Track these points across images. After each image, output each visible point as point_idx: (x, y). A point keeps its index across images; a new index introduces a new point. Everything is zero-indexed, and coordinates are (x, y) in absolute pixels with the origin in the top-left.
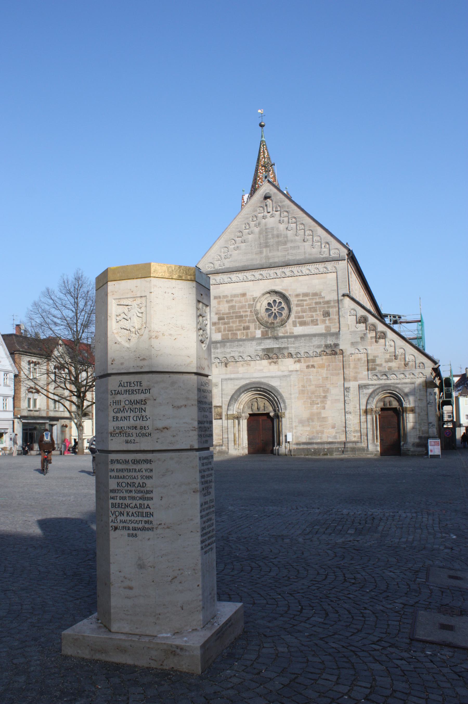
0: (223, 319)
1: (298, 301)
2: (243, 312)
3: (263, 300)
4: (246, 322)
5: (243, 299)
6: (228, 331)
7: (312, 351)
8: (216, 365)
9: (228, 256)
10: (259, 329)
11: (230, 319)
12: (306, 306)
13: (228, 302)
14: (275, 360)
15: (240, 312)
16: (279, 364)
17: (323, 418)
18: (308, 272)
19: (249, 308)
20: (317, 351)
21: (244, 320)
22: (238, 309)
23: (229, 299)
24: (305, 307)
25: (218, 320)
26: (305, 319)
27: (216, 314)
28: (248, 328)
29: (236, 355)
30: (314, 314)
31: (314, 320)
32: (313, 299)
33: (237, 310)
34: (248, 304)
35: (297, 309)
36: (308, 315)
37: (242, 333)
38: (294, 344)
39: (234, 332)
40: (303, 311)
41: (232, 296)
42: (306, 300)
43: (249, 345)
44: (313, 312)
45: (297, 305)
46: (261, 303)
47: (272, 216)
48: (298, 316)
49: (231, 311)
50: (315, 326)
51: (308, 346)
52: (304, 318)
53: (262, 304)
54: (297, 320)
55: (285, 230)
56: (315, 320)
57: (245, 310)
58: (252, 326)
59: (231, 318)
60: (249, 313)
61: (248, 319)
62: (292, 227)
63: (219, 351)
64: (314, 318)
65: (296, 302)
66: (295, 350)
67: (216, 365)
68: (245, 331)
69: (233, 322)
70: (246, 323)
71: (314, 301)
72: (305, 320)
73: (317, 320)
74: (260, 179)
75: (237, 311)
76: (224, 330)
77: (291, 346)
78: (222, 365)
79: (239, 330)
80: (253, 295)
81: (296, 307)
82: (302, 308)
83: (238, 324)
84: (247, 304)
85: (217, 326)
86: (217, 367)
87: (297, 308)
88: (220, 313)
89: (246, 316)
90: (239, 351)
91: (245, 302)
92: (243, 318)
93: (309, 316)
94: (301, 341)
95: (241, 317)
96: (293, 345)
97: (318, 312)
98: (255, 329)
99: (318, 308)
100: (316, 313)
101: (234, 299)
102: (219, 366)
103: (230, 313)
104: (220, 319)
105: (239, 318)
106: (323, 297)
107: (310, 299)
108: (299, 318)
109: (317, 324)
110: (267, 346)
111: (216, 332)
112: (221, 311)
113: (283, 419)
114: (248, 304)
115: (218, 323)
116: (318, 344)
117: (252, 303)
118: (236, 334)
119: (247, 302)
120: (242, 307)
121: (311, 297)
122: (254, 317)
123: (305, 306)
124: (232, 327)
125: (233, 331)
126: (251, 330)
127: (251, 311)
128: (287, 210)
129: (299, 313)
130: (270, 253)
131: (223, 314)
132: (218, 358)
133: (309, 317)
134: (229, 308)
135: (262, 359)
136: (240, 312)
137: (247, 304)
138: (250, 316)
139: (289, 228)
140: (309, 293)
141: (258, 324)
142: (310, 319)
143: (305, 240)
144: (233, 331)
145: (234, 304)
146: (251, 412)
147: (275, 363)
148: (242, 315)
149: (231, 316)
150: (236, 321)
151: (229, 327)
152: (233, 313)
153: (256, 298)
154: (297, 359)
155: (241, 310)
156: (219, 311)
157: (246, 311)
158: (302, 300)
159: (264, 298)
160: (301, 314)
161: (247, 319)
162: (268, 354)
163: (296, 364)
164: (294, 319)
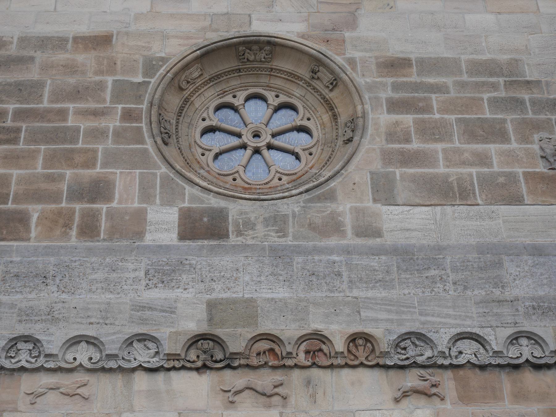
1: (396, 87)
3: (199, 82)
4: (95, 159)
7: (510, 331)
10: (168, 202)
12: (444, 110)
15: (62, 114)
16: (292, 400)
19: (117, 97)
21: (80, 151)
22: (51, 101)
24: (437, 116)
26: (441, 170)
30: (493, 148)
32: (478, 86)
33: (45, 104)
34: (115, 81)
35: (397, 123)
36: (457, 151)
37: (59, 213)
38: (386, 284)
39: (10, 206)
41: (24, 41)
43: (99, 275)
44: (486, 141)
46: (186, 93)
48: (402, 153)
50: (504, 209)
52: (433, 163)
53: (186, 100)
56: (501, 180)
57: (92, 105)
61: (106, 151)
64: (496, 169)
66: (400, 323)
68: (78, 207)
70: (90, 163)
71: (486, 96)
72: (447, 176)
73: (511, 178)
75: (49, 111)
77: (370, 294)
80: (149, 49)
81: (389, 111)
82: (423, 121)
83: (40, 170)
84: (110, 80)
87: (395, 117)
91: (100, 72)
92: (74, 140)
93: (466, 155)
94: (433, 272)
96: (380, 293)
97: (514, 145)
99: (510, 127)
100: (505, 147)
101: (39, 56)
105: (47, 143)
106: (528, 82)
107: (462, 85)
109: (517, 200)
110: (218, 286)
114: (115, 81)
116: (541, 293)
117: (139, 79)
121: (465, 78)
122: (142, 142)
126: (114, 204)
127: (128, 115)
129: (408, 140)
133: (464, 163)
136: (62, 114)
137: (110, 80)
138: (118, 135)
140: (456, 62)
141: (165, 180)
142: (474, 171)
148: (78, 130)
149: (8, 130)
150: (32, 155)
152: (19, 115)
153: (164, 60)
155: (71, 106)
157: (96, 114)
158: (416, 87)
159: (207, 76)
160: (415, 145)
161: (100, 147)
162: (219, 332)
163: (405, 403)
164: (377, 166)
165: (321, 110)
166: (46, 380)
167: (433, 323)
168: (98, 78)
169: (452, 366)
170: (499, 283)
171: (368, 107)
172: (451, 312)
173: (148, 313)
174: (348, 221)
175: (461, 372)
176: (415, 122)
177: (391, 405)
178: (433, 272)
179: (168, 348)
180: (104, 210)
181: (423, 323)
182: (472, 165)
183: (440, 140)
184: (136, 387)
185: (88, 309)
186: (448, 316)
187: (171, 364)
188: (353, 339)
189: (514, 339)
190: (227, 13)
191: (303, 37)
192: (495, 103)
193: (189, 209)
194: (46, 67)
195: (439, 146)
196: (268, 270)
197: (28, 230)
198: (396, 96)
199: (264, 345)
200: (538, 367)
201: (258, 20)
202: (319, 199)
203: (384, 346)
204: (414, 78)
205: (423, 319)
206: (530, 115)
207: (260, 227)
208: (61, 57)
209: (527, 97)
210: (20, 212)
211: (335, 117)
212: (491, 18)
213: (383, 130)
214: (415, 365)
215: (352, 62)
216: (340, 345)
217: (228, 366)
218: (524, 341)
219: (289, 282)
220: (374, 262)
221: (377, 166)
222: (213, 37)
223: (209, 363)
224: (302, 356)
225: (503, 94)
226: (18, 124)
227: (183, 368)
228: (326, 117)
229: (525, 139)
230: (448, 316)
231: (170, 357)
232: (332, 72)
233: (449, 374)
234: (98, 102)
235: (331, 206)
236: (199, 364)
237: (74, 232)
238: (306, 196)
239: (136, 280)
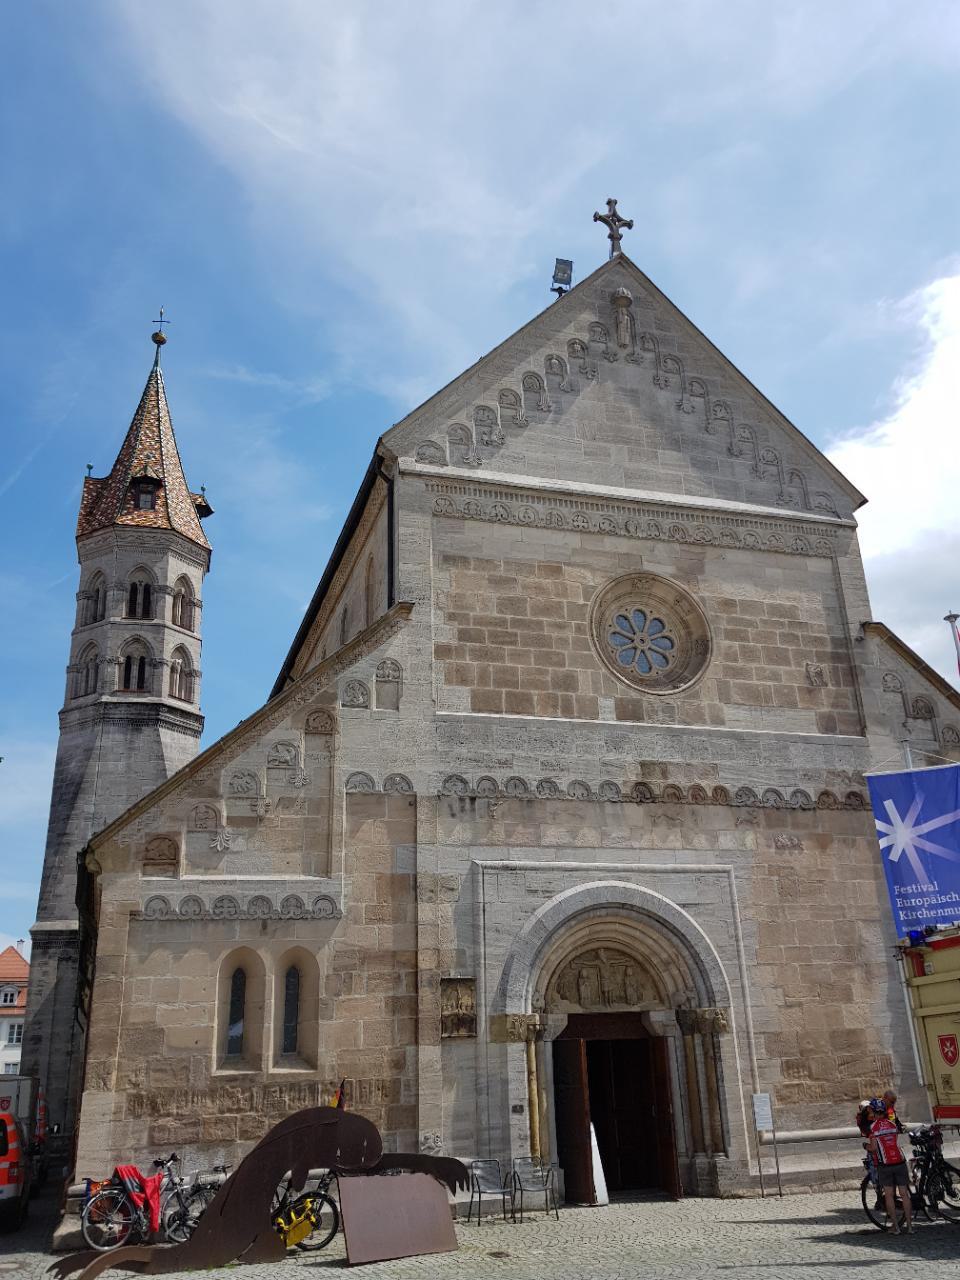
0: (479, 638)
2: (550, 625)
5: (547, 582)
6: (498, 683)
8: (450, 807)
9: (494, 438)
11: (503, 643)
13: (497, 582)
14: (671, 809)
15: (540, 624)
17: (851, 1032)
18: (750, 540)
20: (808, 790)
23: (501, 572)
25: (460, 639)
27: (451, 617)
28: (568, 682)
29: (533, 777)
30: (782, 669)
31: (785, 687)
35: (730, 647)
37: (549, 696)
40: (749, 654)
42: (750, 624)
45: (731, 635)
47: (633, 359)
48: (732, 668)
49: (509, 617)
51: (780, 771)
54: (732, 681)
55: (673, 408)
58: (584, 677)
59: (507, 639)
60: (570, 634)
62: (694, 404)
63: (463, 751)
65: (724, 625)
66: (738, 780)
67: (450, 807)
69: (516, 656)
74: (146, 449)
75: (531, 622)
76: (483, 678)
78: (473, 810)
79: (542, 685)
83: (533, 666)
85: (453, 661)
86: (453, 815)
88: (465, 618)
89: (563, 642)
90: (542, 759)
91: (558, 595)
94: (753, 751)
95: (541, 641)
97: (793, 668)
98: (596, 690)
101: (520, 578)
102: (463, 810)
103: (502, 623)
104: (463, 635)
107: (764, 622)
108: (737, 673)
110: (645, 753)
111: (448, 681)
112: (473, 609)
113: (724, 1039)
115: (459, 652)
117: (581, 602)
118: (528, 699)
119: (565, 595)
120: (547, 610)
122: (589, 650)
123: (753, 640)
124: (514, 671)
125: (515, 685)
127: (579, 629)
128: (677, 354)
129: (736, 660)
130: (630, 460)
131: (479, 621)
132: (464, 782)
133: (765, 678)
134: (498, 605)
135: (628, 799)
139: (686, 406)
143: (735, 450)
144: (515, 685)
145: (518, 592)
146: (578, 1009)
147: (671, 821)
151: (505, 670)
153: (594, 587)
154: (743, 813)
156: (462, 608)
157: (561, 627)
160: (740, 664)
165: (680, 627)
166: (559, 805)
167: (754, 782)
168: (558, 600)
169: (764, 807)
170: (787, 760)
171: (713, 635)
172: (763, 775)
173: (610, 768)
174: (707, 712)
175: (768, 811)
176: (740, 646)
177: (733, 828)
178: (753, 751)
179: (625, 790)
180: (574, 697)
181: (750, 781)
182: (770, 679)
183: (753, 661)
184: (607, 812)
185: (577, 764)
186: (762, 778)
187: (625, 799)
188: (716, 789)
189: (795, 793)
190: (627, 554)
191: (673, 576)
192: (782, 635)
193: (621, 699)
194: (525, 587)
195: (754, 665)
196: (670, 744)
197: (534, 708)
198: (729, 627)
199: (671, 791)
200: (804, 809)
201: (647, 561)
202: (689, 697)
203: (732, 795)
204: (738, 616)
205: (750, 779)
206: (802, 647)
207: (660, 713)
208: (532, 580)
209: (800, 634)
210: (527, 694)
211: (689, 634)
212: (780, 571)
213: (723, 651)
214: (746, 806)
215: (703, 599)
216: (710, 794)
217: (653, 802)
218: (799, 795)
219: (682, 752)
220: (724, 742)
221: (721, 676)
222: (621, 572)
223: (643, 800)
224: (690, 797)
225: (786, 630)
226: (515, 630)
227: (631, 802)
228: (683, 632)
229: (799, 664)
230: (762, 778)
231: (626, 796)
232: (691, 605)
233: (761, 811)
234: (560, 618)
235: (696, 702)
236: (639, 800)
237: (559, 711)
238: (683, 694)
239: (601, 747)
